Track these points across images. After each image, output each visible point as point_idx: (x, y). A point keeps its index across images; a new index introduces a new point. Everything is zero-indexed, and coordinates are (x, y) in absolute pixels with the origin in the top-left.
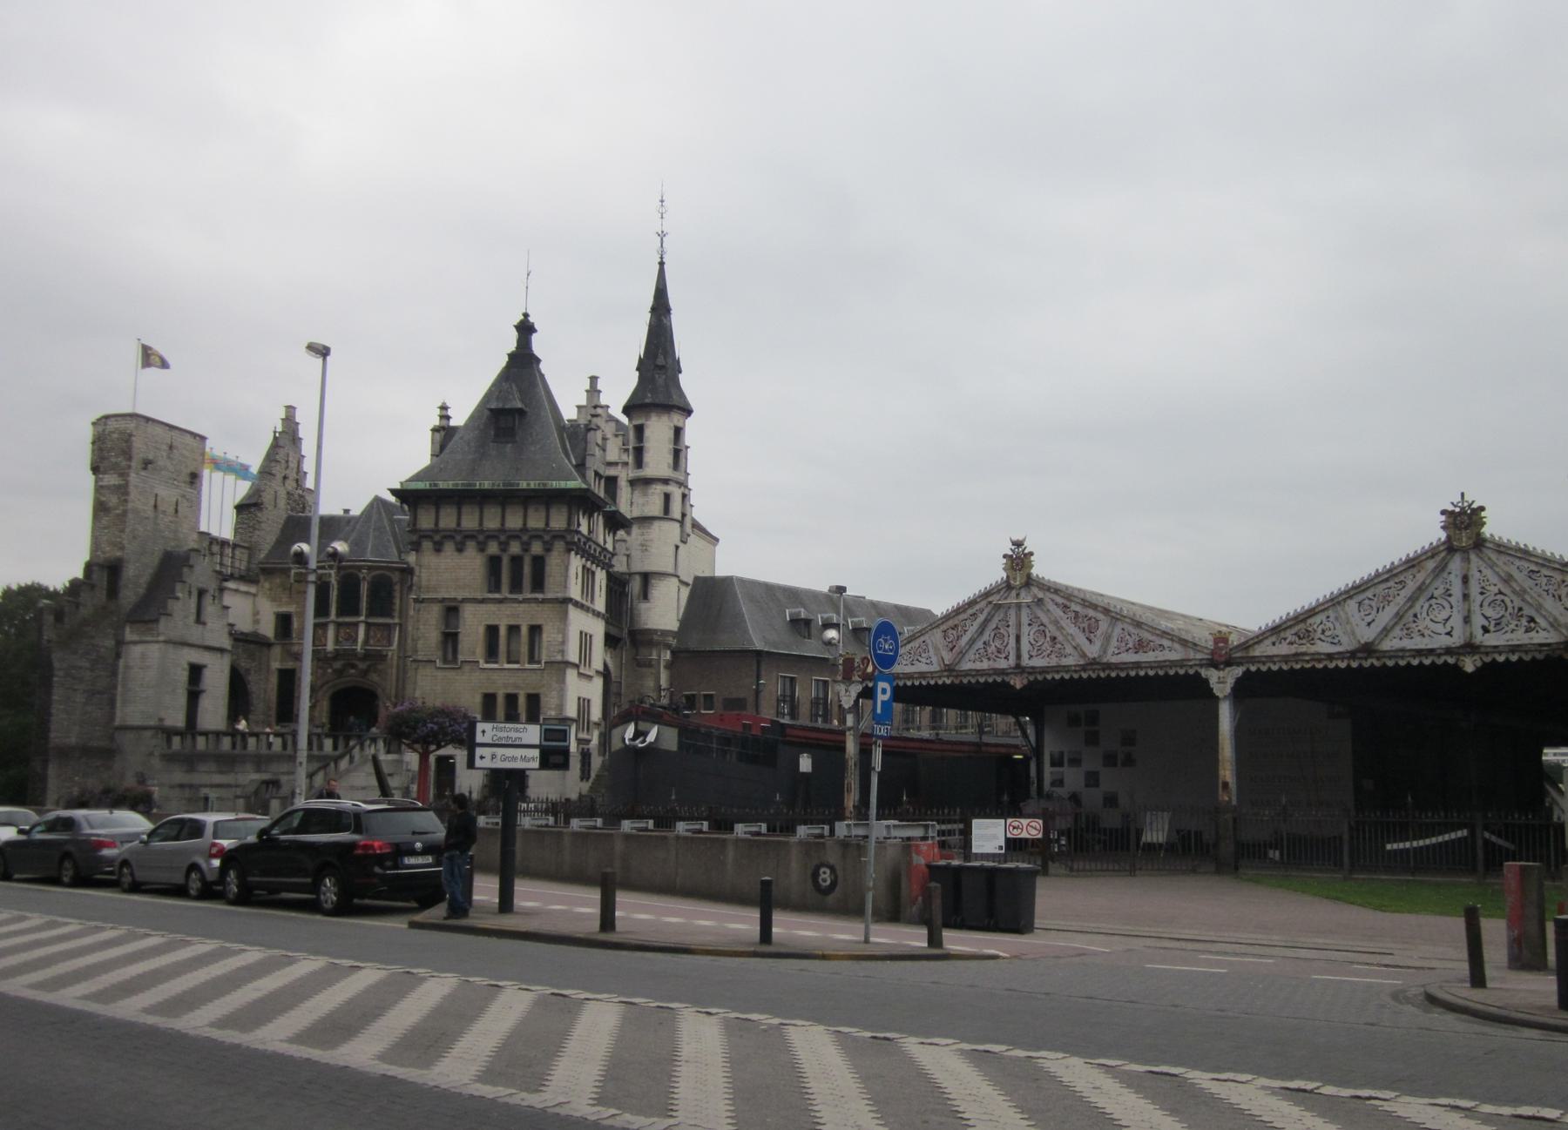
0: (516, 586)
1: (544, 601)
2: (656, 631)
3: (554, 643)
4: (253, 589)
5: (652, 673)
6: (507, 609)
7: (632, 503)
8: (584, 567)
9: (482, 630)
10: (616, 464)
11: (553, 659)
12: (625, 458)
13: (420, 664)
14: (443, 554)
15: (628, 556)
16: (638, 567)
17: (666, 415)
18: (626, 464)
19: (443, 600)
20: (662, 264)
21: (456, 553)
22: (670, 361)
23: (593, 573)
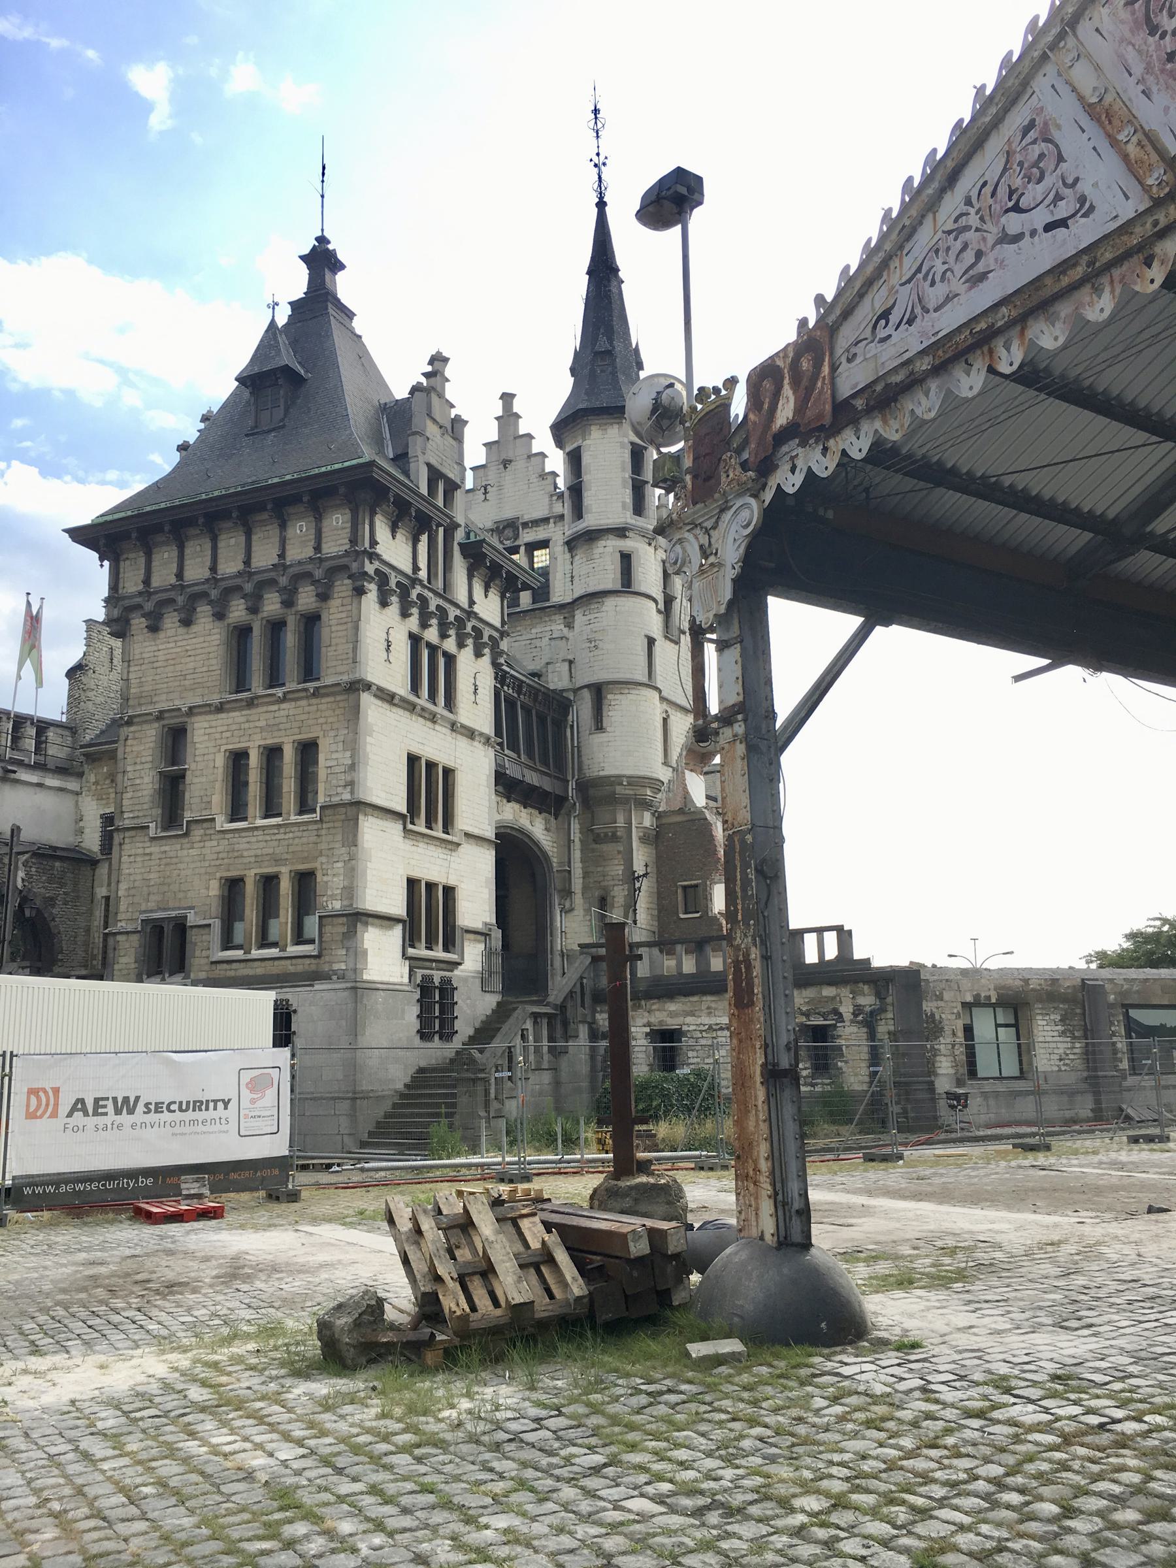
0: (274, 678)
1: (317, 693)
2: (617, 780)
3: (337, 770)
4: (72, 784)
5: (619, 852)
6: (261, 716)
7: (572, 577)
8: (415, 639)
9: (220, 760)
10: (546, 520)
11: (336, 800)
12: (558, 508)
13: (127, 834)
14: (162, 635)
15: (571, 662)
16: (585, 677)
17: (616, 426)
18: (562, 517)
19: (160, 716)
20: (601, 205)
21: (182, 630)
22: (618, 346)
23: (450, 659)
